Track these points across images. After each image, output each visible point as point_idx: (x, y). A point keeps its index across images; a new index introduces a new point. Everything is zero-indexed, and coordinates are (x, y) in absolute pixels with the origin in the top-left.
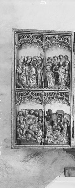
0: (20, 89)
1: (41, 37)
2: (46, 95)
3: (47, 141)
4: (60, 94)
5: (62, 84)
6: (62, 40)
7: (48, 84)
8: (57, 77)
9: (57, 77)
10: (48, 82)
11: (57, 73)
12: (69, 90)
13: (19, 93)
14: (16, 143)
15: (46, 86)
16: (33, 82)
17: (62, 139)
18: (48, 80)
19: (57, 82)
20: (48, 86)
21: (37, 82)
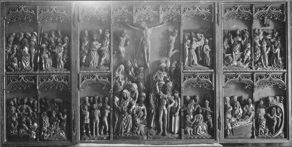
0: (12, 73)
1: (35, 9)
2: (41, 80)
3: (43, 136)
4: (58, 78)
5: (60, 67)
6: (60, 11)
7: (44, 67)
8: (54, 57)
9: (54, 57)
10: (43, 63)
11: (54, 53)
12: (69, 72)
13: (10, 78)
14: (6, 139)
15: (41, 69)
16: (26, 64)
17: (61, 134)
18: (43, 62)
19: (55, 64)
20: (44, 69)
21: (31, 64)
